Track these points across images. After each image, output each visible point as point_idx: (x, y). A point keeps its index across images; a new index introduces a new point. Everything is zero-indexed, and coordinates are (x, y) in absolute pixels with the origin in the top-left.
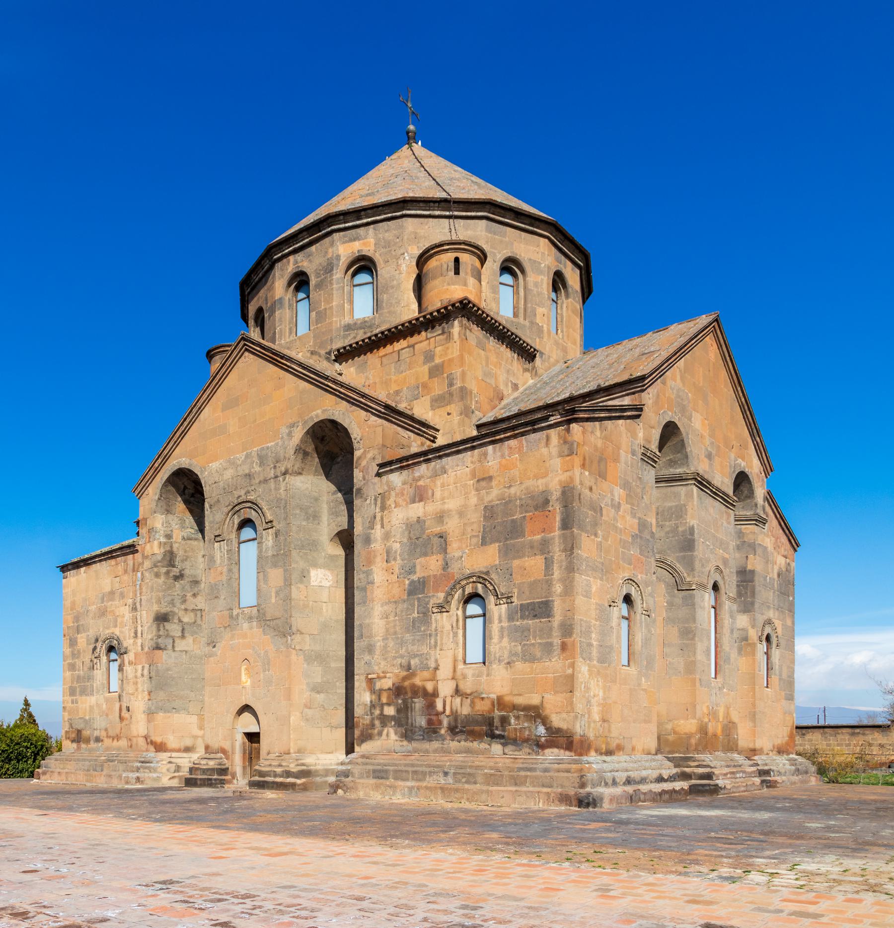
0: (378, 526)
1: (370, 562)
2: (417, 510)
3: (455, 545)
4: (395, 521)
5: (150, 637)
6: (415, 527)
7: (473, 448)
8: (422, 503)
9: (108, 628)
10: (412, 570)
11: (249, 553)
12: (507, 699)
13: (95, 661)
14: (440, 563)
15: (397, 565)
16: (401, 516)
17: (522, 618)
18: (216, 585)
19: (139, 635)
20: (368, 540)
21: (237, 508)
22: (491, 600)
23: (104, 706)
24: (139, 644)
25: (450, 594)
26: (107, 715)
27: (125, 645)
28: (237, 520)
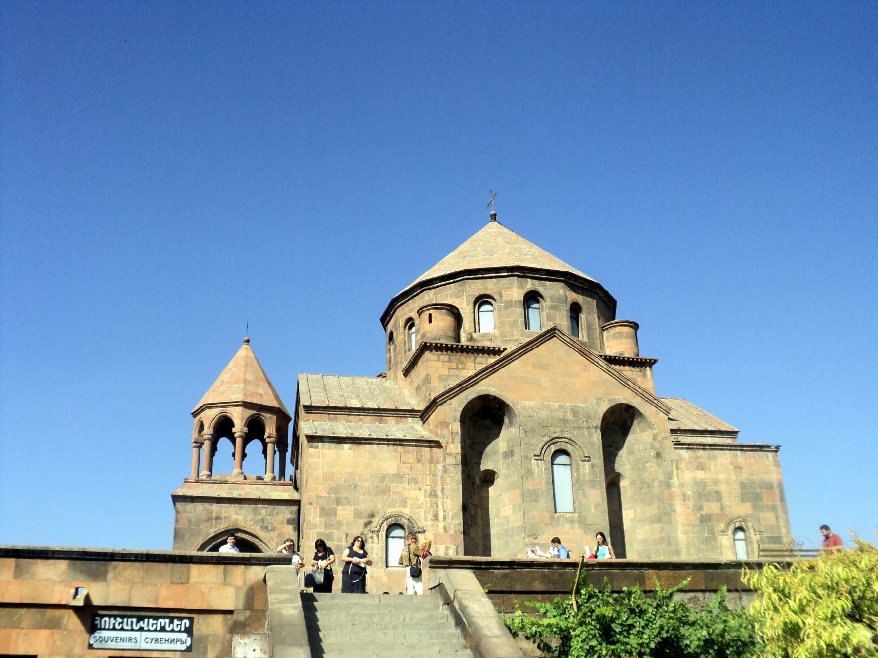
0: (675, 478)
2: (700, 475)
3: (726, 499)
4: (686, 477)
5: (457, 522)
6: (702, 484)
7: (731, 450)
8: (703, 472)
9: (392, 507)
10: (701, 508)
11: (563, 474)
13: (370, 535)
14: (719, 507)
15: (691, 503)
16: (690, 475)
17: (770, 543)
18: (534, 491)
19: (441, 517)
20: (668, 485)
21: (556, 440)
23: (385, 579)
27: (420, 525)
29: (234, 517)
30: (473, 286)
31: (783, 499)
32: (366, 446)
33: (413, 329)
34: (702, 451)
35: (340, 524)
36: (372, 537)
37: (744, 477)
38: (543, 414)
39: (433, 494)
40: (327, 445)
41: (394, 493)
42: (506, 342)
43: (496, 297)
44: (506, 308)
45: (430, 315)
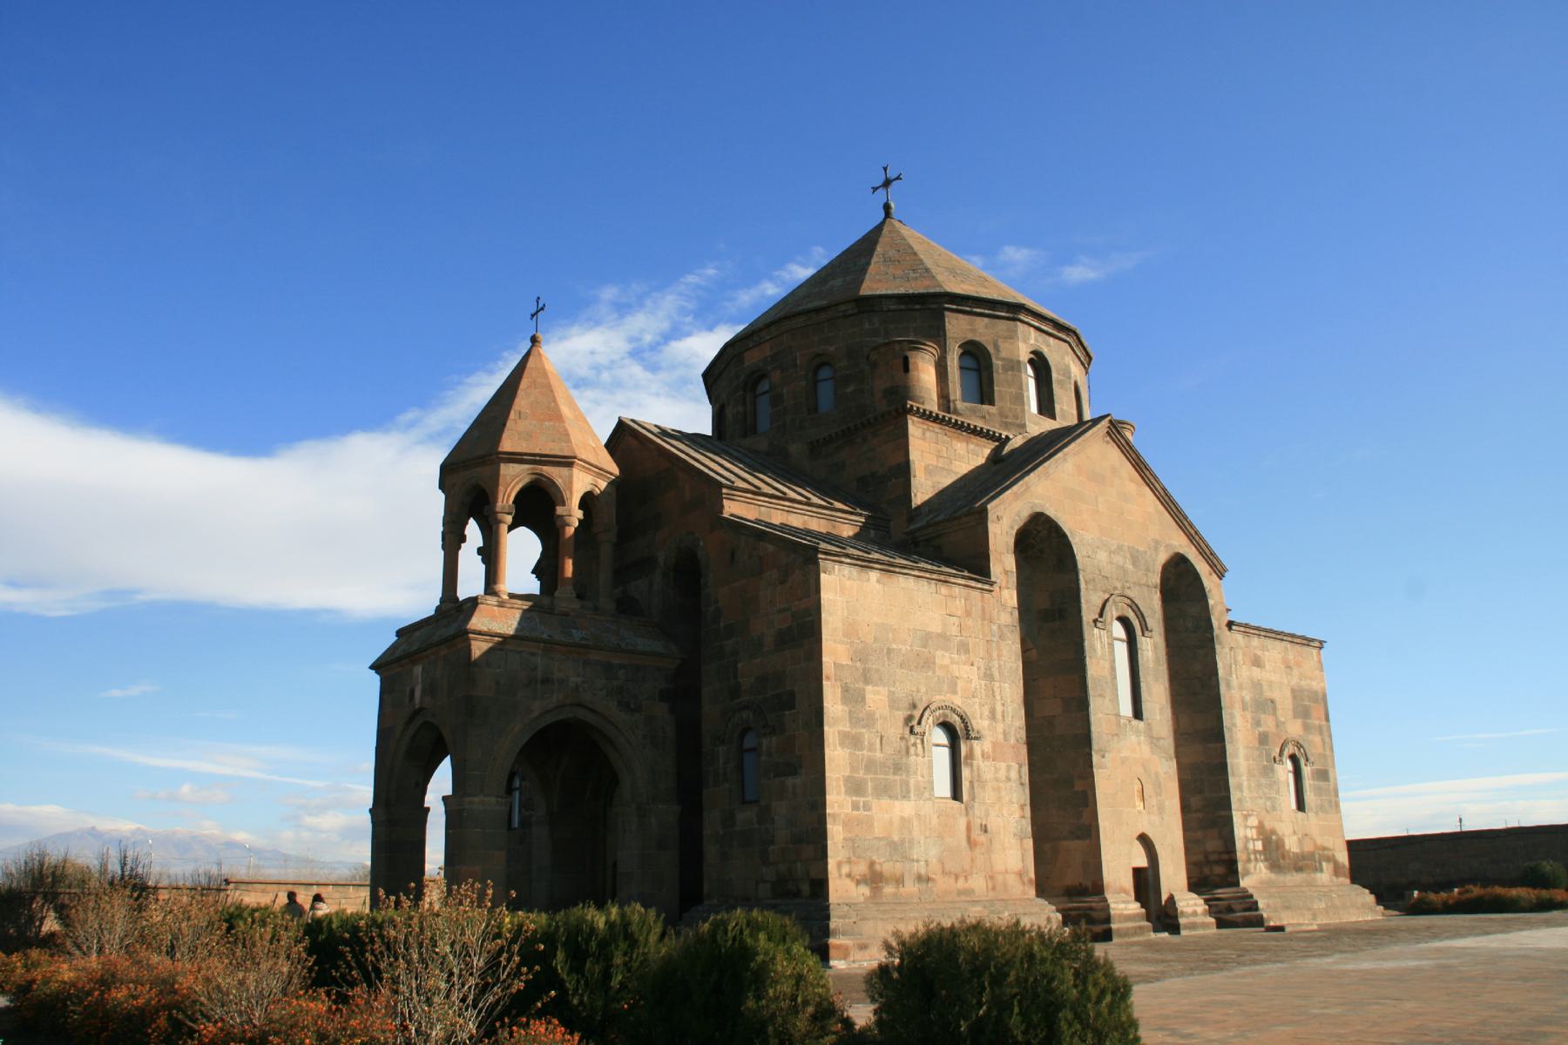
1: (1232, 706)
2: (1256, 673)
6: (1257, 686)
9: (940, 692)
10: (1258, 723)
12: (1319, 842)
13: (912, 739)
15: (1249, 715)
19: (999, 716)
20: (1228, 685)
22: (1302, 761)
23: (935, 820)
24: (1000, 730)
25: (1281, 751)
26: (940, 836)
28: (1115, 614)
29: (574, 680)
30: (954, 322)
31: (1327, 719)
32: (901, 578)
33: (825, 373)
34: (1255, 641)
35: (870, 721)
36: (915, 744)
37: (1294, 681)
38: (1102, 556)
39: (988, 676)
40: (846, 570)
41: (942, 667)
42: (1006, 426)
43: (991, 349)
44: (1005, 370)
45: (906, 361)
